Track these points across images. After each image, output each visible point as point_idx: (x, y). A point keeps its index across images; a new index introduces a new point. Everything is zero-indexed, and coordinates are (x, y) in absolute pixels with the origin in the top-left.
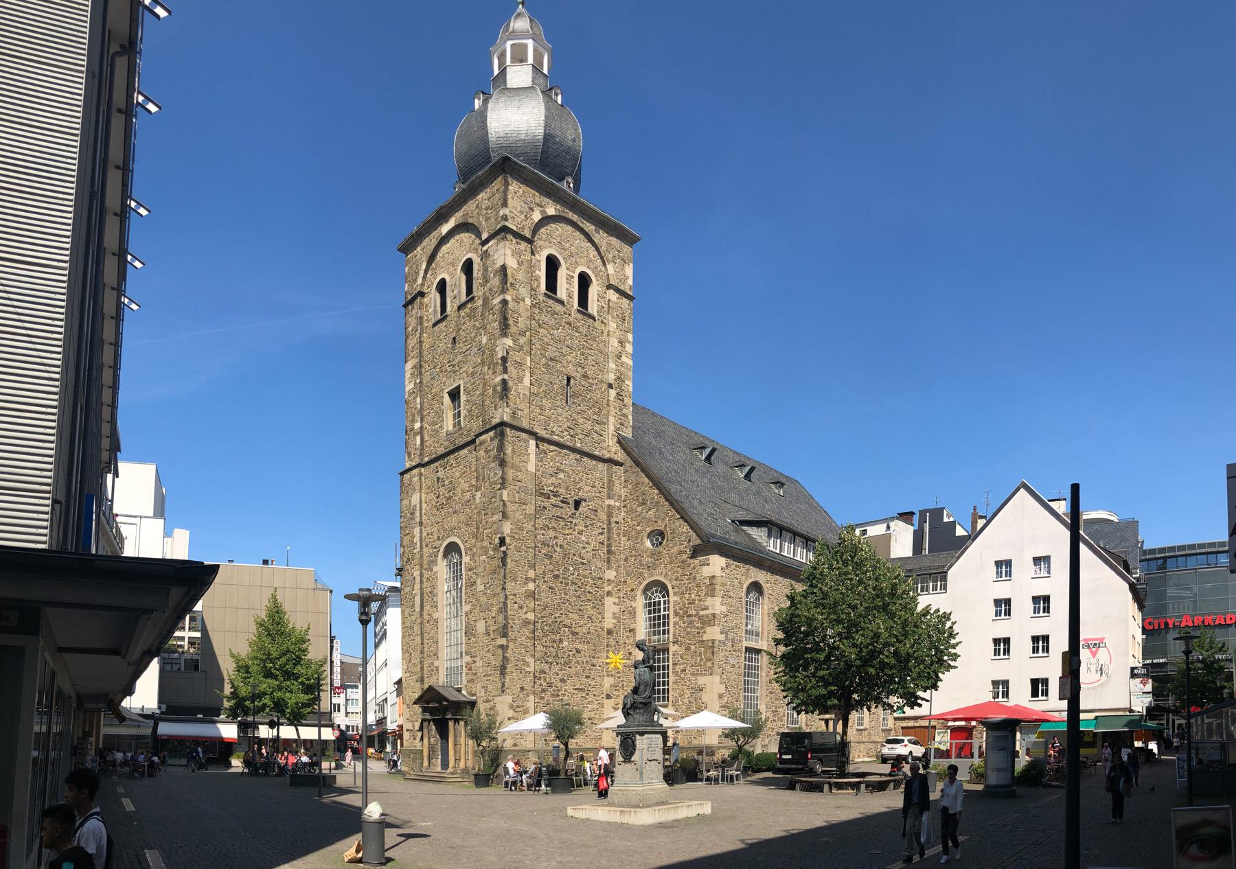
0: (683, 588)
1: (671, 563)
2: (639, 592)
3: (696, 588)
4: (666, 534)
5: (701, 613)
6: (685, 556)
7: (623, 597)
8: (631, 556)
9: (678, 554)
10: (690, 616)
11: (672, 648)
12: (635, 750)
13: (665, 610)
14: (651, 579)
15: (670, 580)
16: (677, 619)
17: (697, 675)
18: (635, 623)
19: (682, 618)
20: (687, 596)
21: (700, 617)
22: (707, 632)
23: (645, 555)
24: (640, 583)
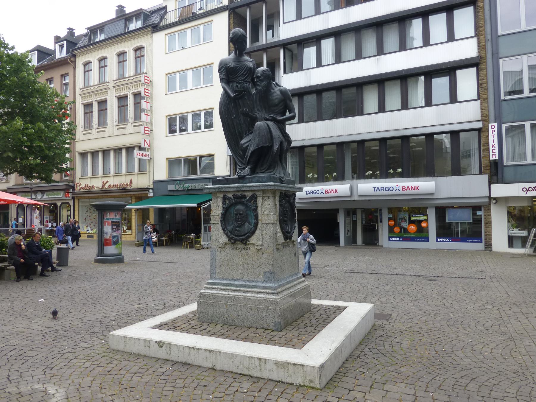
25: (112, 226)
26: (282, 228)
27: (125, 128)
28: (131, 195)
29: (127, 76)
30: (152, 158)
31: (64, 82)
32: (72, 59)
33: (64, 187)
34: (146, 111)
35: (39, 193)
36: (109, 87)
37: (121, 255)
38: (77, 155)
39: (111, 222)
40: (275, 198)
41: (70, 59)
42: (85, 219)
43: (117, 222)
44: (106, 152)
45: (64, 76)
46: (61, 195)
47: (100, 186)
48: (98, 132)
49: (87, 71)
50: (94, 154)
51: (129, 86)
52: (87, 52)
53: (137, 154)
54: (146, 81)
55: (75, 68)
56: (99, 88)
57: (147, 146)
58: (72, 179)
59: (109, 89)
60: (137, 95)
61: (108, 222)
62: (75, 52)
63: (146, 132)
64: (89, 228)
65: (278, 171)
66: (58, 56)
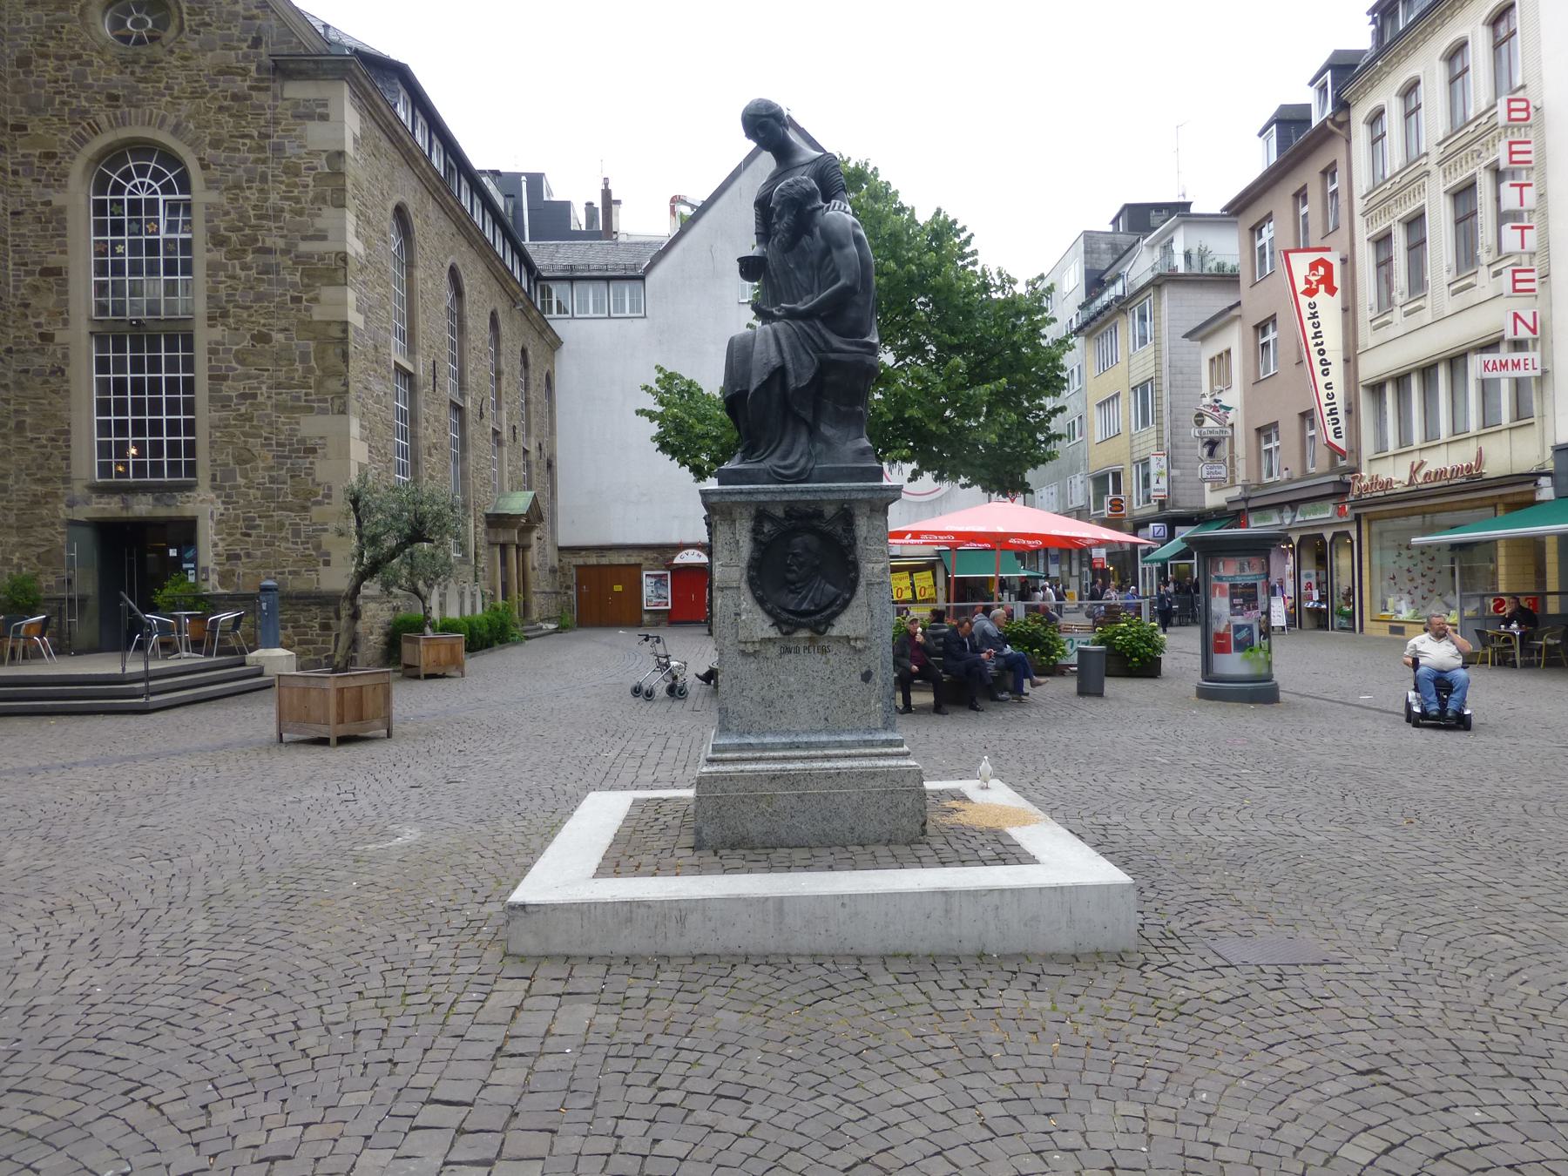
0: (240, 172)
1: (196, 95)
2: (78, 170)
3: (284, 178)
4: (175, 10)
5: (304, 247)
6: (242, 85)
7: (15, 173)
8: (45, 56)
9: (221, 73)
10: (268, 251)
11: (204, 337)
12: (852, 586)
13: (172, 227)
14: (125, 133)
15: (194, 144)
16: (220, 255)
17: (293, 409)
18: (64, 252)
19: (236, 254)
20: (252, 195)
21: (300, 259)
22: (323, 298)
23: (96, 61)
24: (83, 141)
25: (1233, 596)
26: (761, 601)
27: (1471, 286)
28: (1495, 501)
29: (1471, 117)
30: (1548, 367)
31: (1331, 189)
32: (1339, 118)
33: (1329, 490)
34: (1526, 215)
35: (1287, 508)
36: (1428, 168)
37: (1270, 680)
38: (1361, 390)
39: (1227, 585)
40: (734, 521)
41: (1333, 120)
42: (1394, 578)
43: (1246, 586)
44: (1427, 371)
45: (1329, 172)
46: (1326, 512)
47: (1405, 477)
48: (1407, 314)
49: (1376, 140)
50: (1401, 380)
51: (1476, 147)
52: (1372, 83)
53: (1486, 366)
54: (1515, 115)
55: (1348, 141)
56: (1405, 181)
57: (1524, 333)
58: (1354, 464)
59: (1427, 173)
60: (1498, 174)
61: (1221, 587)
62: (1345, 95)
63: (1519, 286)
64: (1403, 606)
65: (778, 453)
66: (1316, 120)
